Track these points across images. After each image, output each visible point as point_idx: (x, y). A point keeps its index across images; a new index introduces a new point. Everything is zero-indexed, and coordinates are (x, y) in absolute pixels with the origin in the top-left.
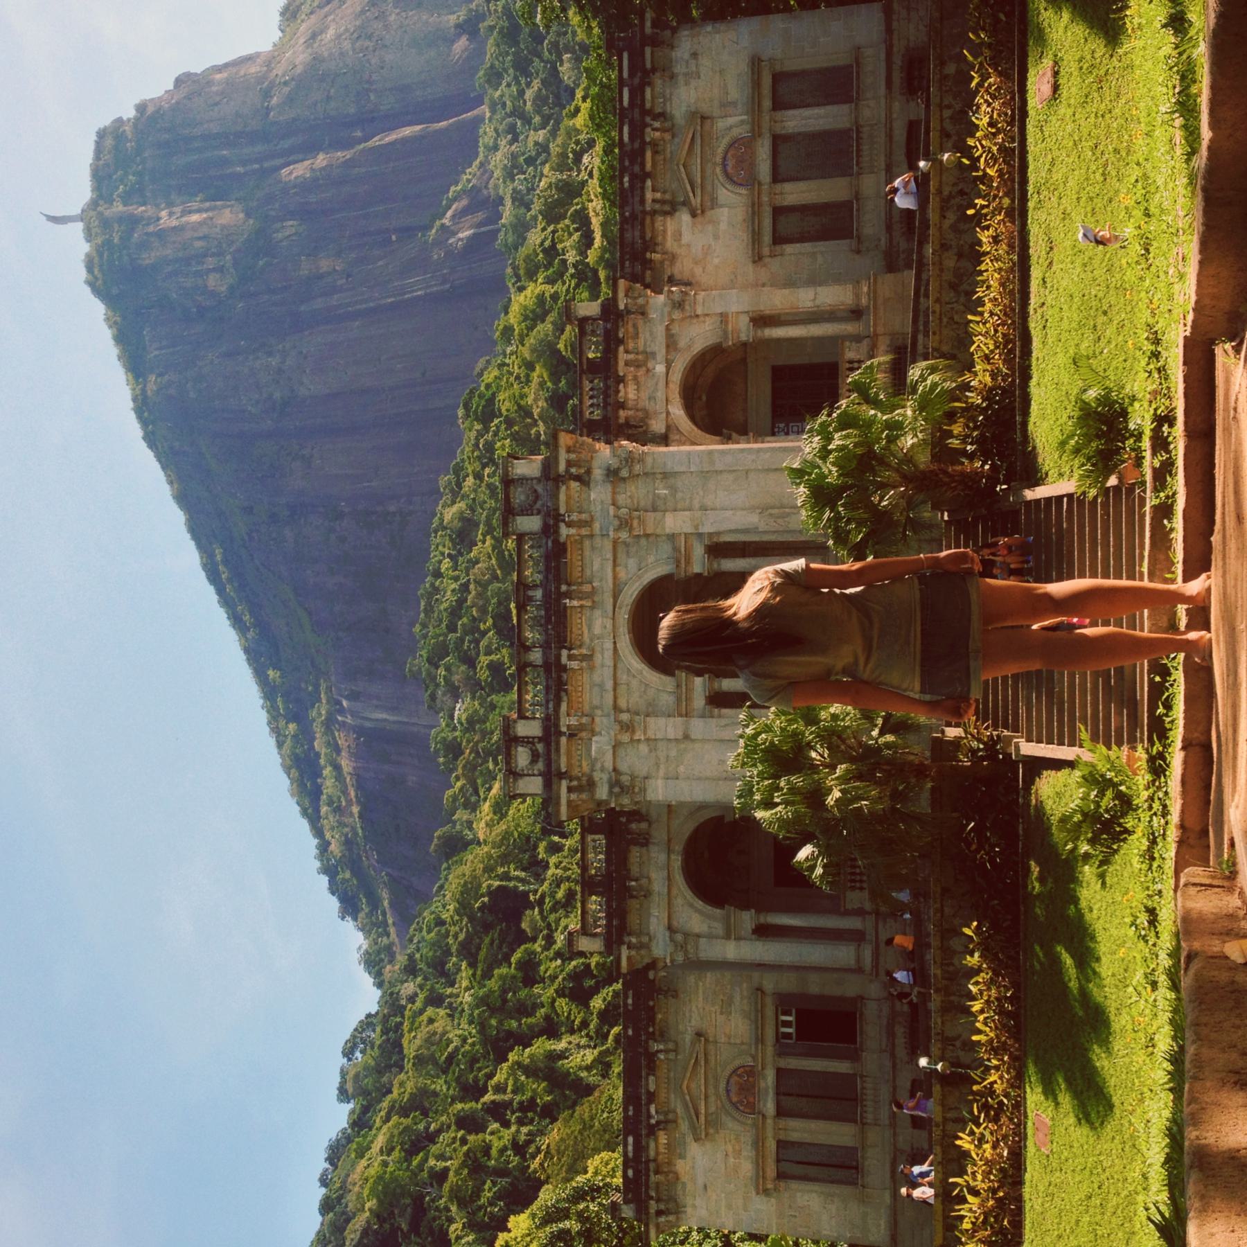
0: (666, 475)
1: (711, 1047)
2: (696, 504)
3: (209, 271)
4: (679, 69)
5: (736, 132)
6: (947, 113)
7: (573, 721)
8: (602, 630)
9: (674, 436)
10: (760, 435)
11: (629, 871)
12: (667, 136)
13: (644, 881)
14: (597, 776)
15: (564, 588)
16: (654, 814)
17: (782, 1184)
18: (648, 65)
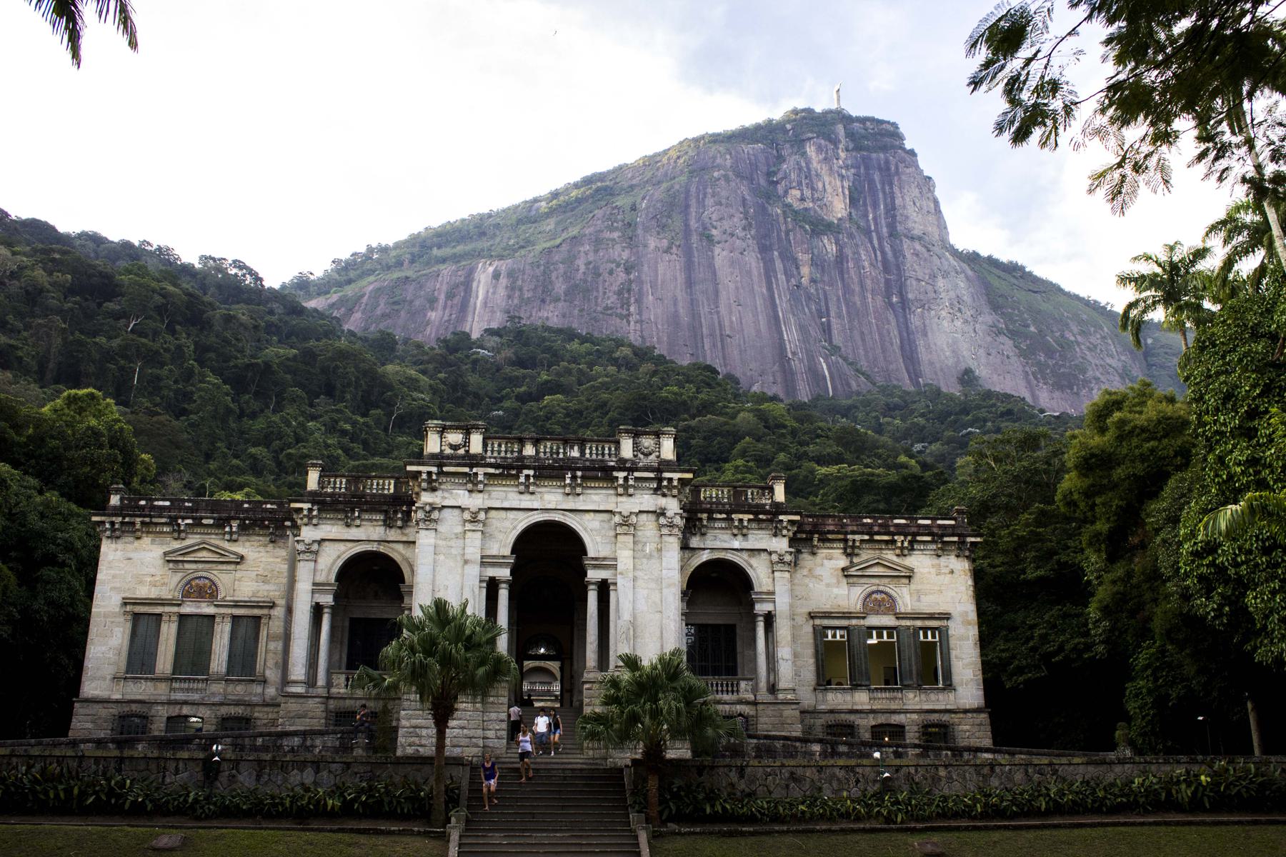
0: (660, 550)
1: (232, 567)
2: (639, 574)
4: (943, 560)
5: (899, 601)
6: (912, 770)
7: (480, 478)
8: (550, 501)
9: (687, 553)
10: (687, 616)
11: (366, 511)
12: (898, 551)
13: (358, 522)
14: (439, 493)
15: (579, 473)
16: (407, 531)
17: (129, 617)
18: (946, 539)
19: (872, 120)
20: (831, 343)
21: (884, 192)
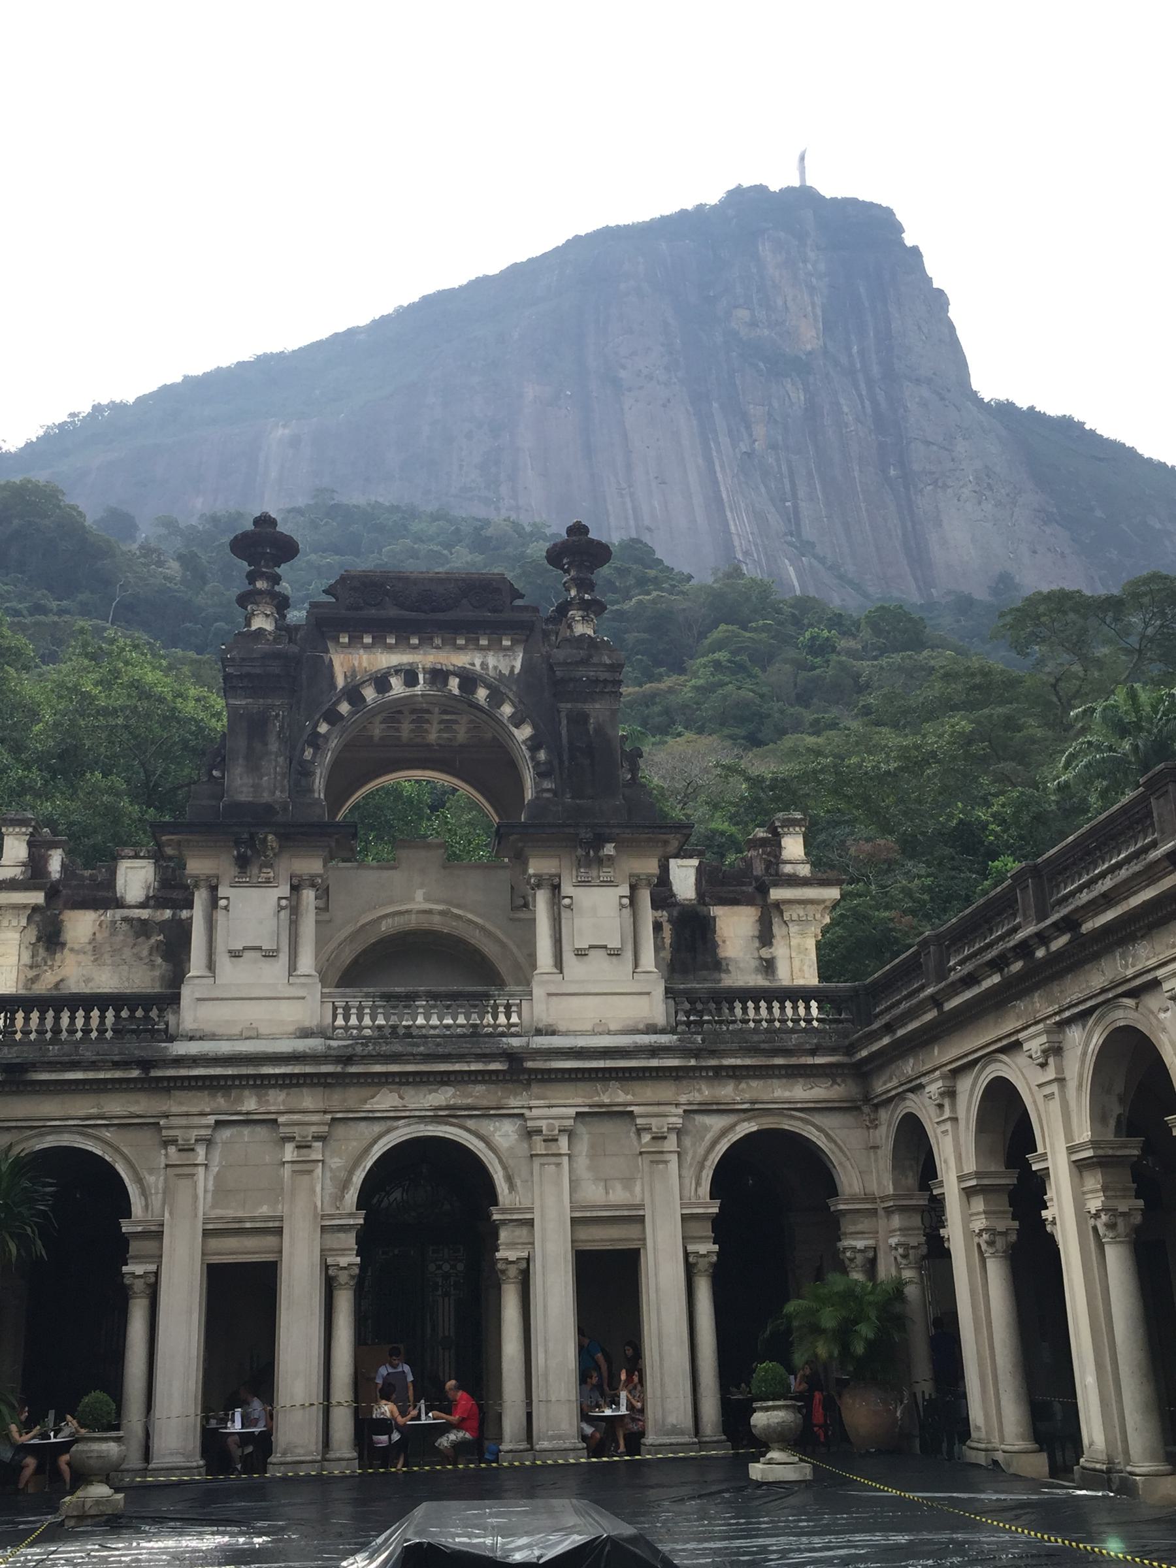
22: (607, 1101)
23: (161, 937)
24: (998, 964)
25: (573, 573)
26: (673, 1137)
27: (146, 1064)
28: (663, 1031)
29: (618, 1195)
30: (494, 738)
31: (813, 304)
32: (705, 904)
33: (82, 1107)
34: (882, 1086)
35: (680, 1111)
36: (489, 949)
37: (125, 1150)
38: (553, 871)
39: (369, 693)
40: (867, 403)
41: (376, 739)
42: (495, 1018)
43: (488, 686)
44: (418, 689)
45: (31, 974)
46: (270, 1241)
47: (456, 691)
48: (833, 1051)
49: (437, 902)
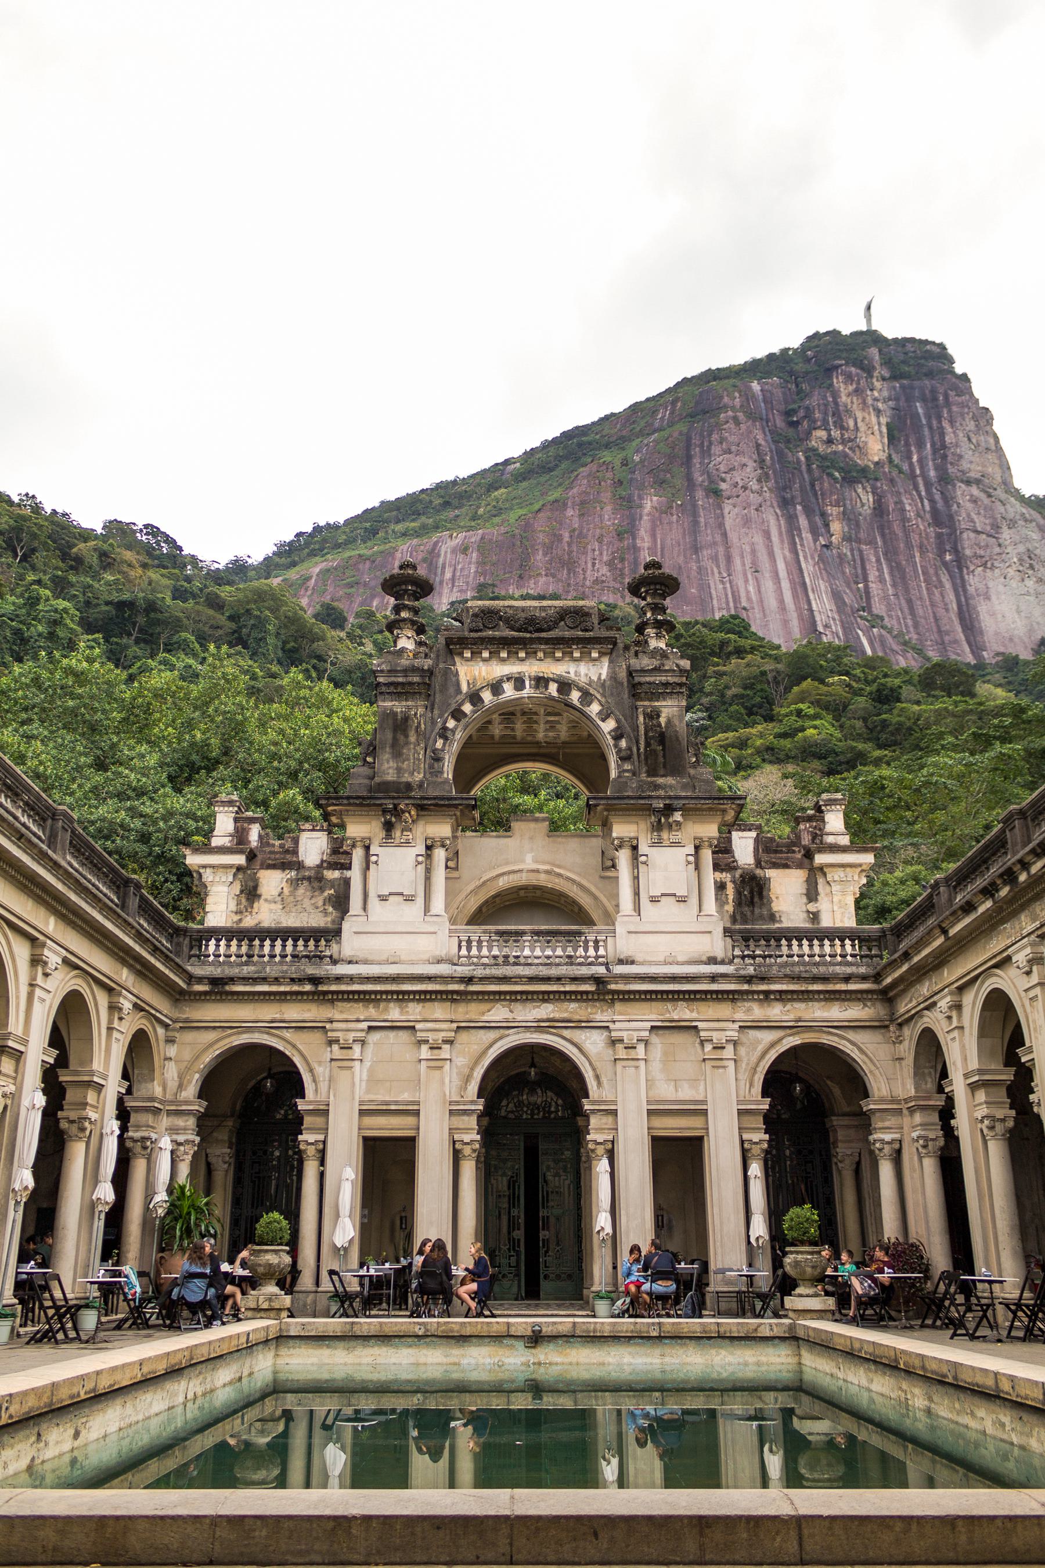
3: (829, 431)
19: (912, 340)
20: (870, 612)
21: (931, 428)
22: (676, 1017)
23: (332, 892)
24: (988, 891)
25: (649, 599)
26: (730, 1048)
27: (315, 980)
28: (722, 962)
29: (687, 1093)
30: (590, 735)
31: (879, 424)
32: (762, 868)
33: (268, 1012)
34: (904, 1007)
35: (736, 1026)
36: (584, 900)
37: (300, 1047)
38: (632, 835)
39: (487, 696)
40: (926, 502)
41: (497, 737)
42: (586, 950)
43: (580, 689)
44: (528, 691)
45: (236, 918)
46: (410, 1120)
47: (555, 694)
48: (864, 978)
49: (544, 863)
